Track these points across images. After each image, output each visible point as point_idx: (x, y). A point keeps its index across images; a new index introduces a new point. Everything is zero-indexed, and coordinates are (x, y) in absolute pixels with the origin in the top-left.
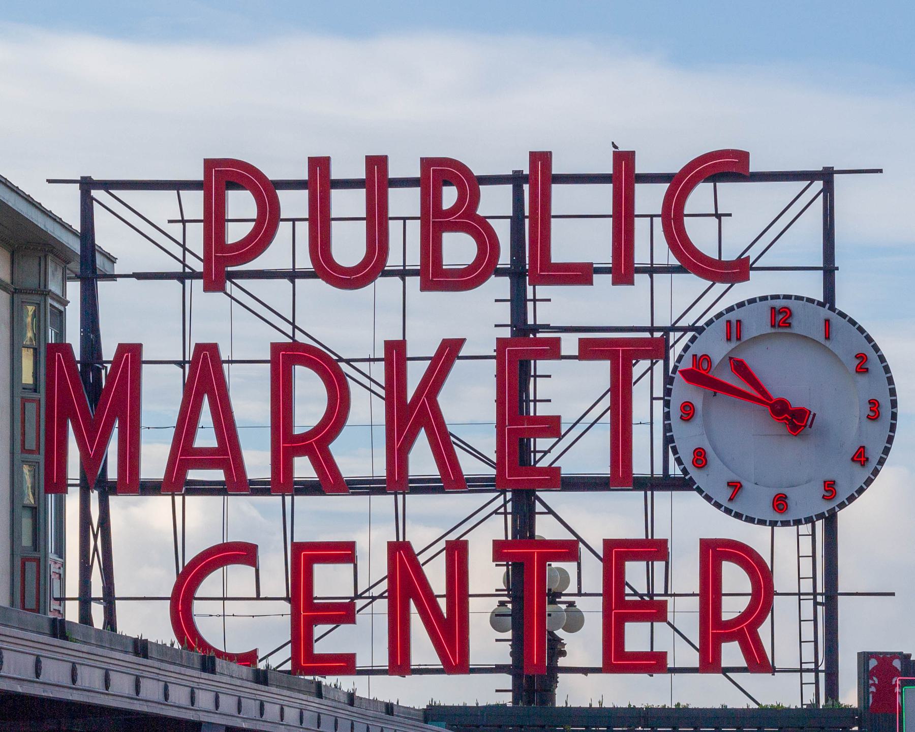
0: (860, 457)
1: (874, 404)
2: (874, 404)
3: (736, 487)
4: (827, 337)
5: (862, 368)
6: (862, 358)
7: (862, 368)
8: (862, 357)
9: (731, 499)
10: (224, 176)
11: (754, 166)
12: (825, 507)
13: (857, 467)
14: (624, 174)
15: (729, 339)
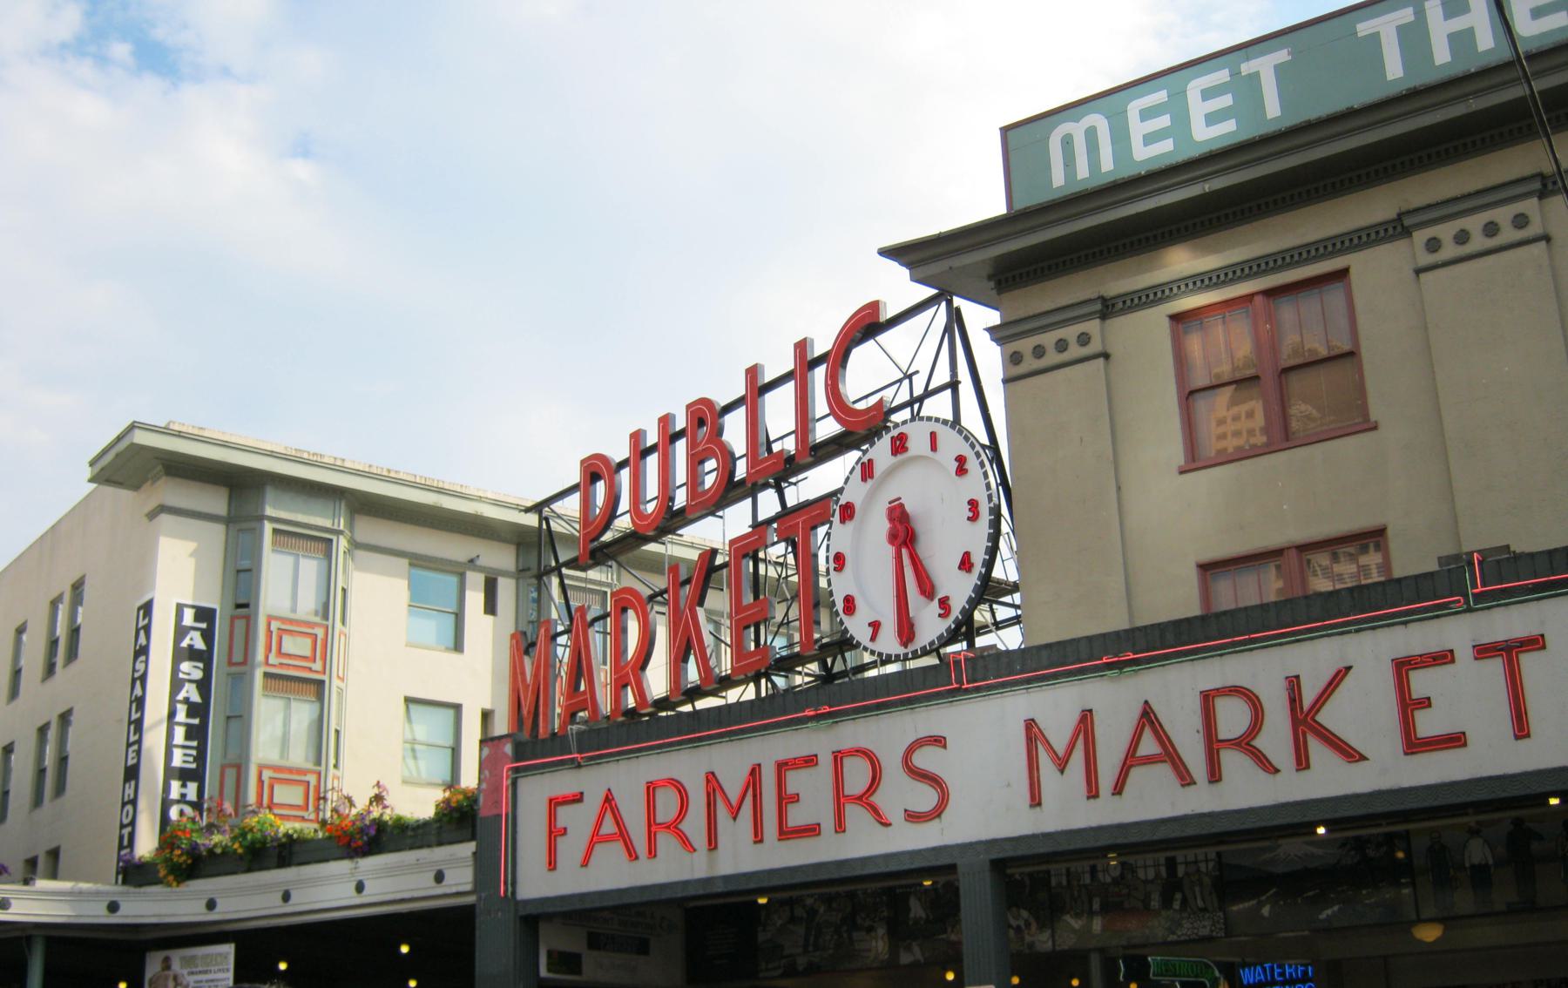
0: (966, 564)
1: (973, 505)
2: (973, 505)
3: (875, 626)
4: (934, 448)
5: (961, 471)
6: (961, 460)
7: (961, 471)
8: (961, 460)
9: (873, 639)
10: (595, 469)
11: (889, 312)
12: (941, 627)
13: (963, 574)
14: (805, 362)
15: (864, 479)
